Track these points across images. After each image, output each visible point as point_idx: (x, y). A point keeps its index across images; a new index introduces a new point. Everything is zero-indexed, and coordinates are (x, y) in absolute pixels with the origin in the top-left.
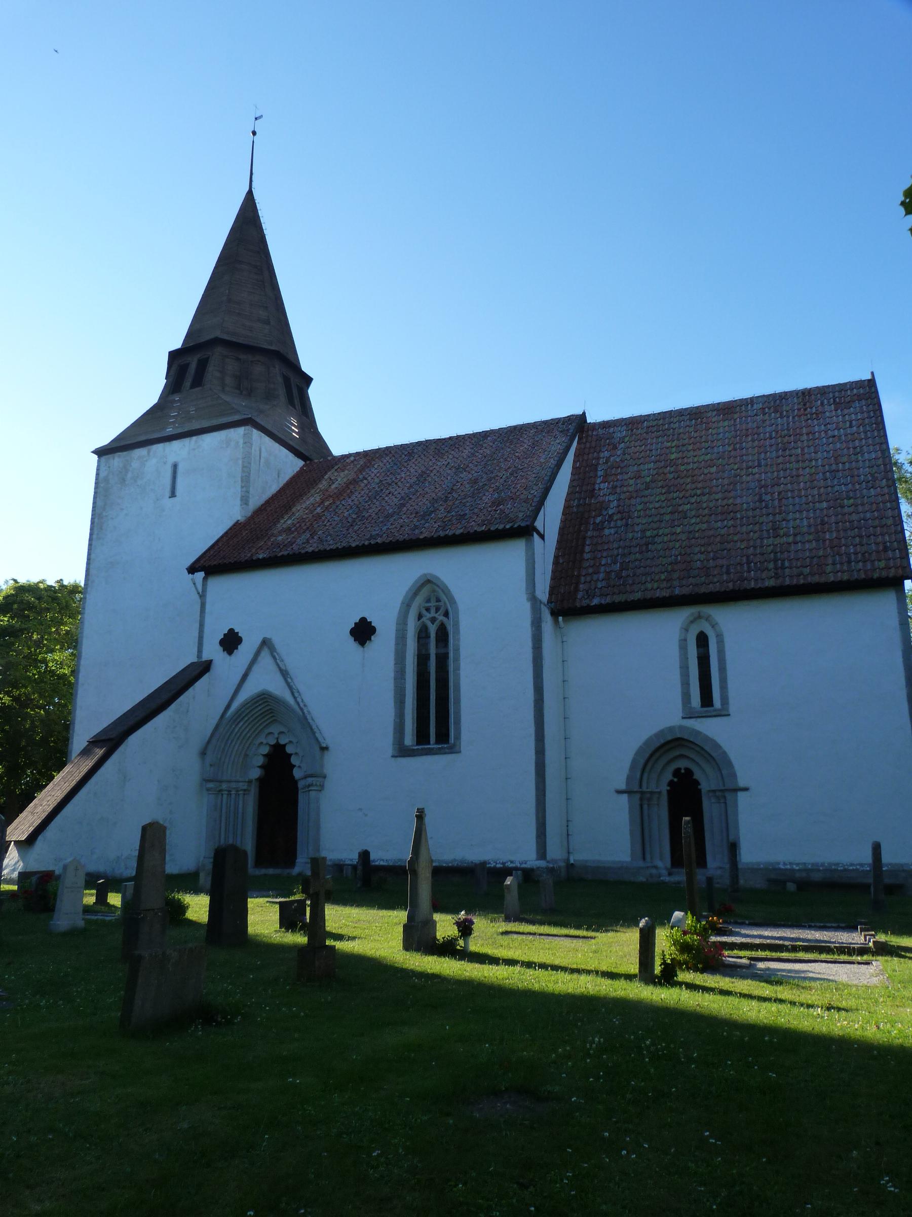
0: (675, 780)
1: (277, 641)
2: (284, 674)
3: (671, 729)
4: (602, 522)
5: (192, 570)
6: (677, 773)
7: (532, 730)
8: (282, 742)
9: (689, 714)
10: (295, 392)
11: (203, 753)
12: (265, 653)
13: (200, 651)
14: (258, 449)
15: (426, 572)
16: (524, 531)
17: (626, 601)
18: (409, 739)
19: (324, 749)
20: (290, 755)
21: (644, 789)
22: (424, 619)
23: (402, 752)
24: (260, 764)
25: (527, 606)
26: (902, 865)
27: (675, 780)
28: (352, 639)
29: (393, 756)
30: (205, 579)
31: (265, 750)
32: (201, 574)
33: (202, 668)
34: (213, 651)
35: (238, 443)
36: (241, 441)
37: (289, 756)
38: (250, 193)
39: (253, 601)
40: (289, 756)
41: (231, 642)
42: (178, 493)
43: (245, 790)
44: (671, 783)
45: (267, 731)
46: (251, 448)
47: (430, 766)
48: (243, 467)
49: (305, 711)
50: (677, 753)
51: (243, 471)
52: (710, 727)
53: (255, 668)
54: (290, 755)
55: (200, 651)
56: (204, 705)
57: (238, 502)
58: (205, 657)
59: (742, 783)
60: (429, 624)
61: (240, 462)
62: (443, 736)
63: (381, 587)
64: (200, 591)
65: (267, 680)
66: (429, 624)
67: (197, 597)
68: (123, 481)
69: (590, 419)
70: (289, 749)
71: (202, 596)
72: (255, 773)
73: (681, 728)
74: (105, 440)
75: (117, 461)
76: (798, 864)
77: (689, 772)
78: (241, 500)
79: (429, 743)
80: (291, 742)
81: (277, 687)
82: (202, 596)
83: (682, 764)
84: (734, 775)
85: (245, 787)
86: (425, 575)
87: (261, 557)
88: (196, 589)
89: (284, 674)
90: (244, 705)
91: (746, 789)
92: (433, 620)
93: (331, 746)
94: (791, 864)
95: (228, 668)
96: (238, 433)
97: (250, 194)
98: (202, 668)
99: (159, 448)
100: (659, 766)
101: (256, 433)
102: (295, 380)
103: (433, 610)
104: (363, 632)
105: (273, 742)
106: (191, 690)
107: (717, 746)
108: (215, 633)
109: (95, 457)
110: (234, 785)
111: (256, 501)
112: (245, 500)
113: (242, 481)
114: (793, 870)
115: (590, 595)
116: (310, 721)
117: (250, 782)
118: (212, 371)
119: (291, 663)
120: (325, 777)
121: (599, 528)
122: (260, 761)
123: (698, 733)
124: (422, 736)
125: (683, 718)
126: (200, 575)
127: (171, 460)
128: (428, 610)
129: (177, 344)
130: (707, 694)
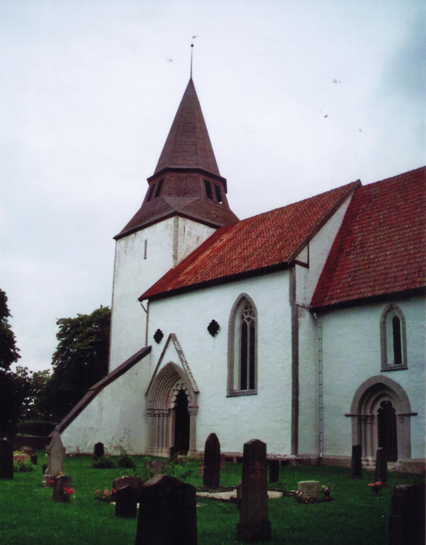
0: (382, 408)
2: (180, 352)
3: (375, 378)
4: (350, 251)
5: (141, 299)
7: (290, 381)
8: (184, 388)
9: (386, 368)
10: (213, 190)
11: (147, 395)
12: (171, 342)
13: (147, 342)
14: (183, 227)
16: (284, 266)
17: (342, 302)
18: (236, 387)
19: (197, 393)
20: (187, 396)
21: (363, 414)
22: (244, 319)
23: (232, 394)
24: (174, 401)
27: (382, 408)
28: (208, 332)
29: (227, 397)
30: (148, 304)
31: (176, 393)
32: (147, 301)
33: (147, 351)
34: (152, 342)
35: (171, 226)
36: (173, 225)
37: (186, 396)
38: (191, 82)
40: (186, 396)
41: (159, 336)
42: (147, 256)
43: (167, 414)
45: (176, 383)
46: (178, 228)
47: (244, 402)
48: (174, 239)
49: (188, 372)
50: (381, 392)
51: (174, 241)
52: (397, 377)
53: (167, 350)
54: (187, 396)
55: (147, 342)
56: (146, 370)
57: (172, 258)
58: (149, 345)
60: (246, 321)
61: (172, 236)
62: (253, 386)
63: (219, 303)
64: (146, 309)
65: (171, 357)
66: (246, 321)
67: (145, 312)
68: (126, 251)
69: (364, 183)
70: (187, 393)
71: (147, 312)
72: (172, 405)
73: (381, 377)
74: (118, 231)
75: (122, 242)
77: (390, 404)
78: (173, 257)
79: (246, 389)
80: (186, 389)
81: (176, 360)
82: (147, 312)
83: (386, 399)
84: (409, 406)
85: (167, 413)
86: (242, 294)
87: (168, 290)
88: (144, 309)
89: (180, 352)
90: (163, 370)
92: (249, 319)
93: (201, 391)
95: (157, 349)
96: (171, 221)
97: (191, 82)
98: (147, 351)
99: (139, 233)
100: (371, 402)
101: (180, 219)
102: (212, 182)
103: (248, 313)
104: (213, 328)
105: (179, 388)
106: (139, 363)
107: (399, 387)
109: (115, 240)
110: (161, 412)
111: (182, 256)
112: (175, 257)
113: (173, 247)
115: (331, 299)
116: (190, 378)
117: (170, 410)
118: (165, 187)
120: (197, 408)
121: (348, 254)
122: (174, 399)
123: (390, 380)
124: (243, 386)
125: (382, 371)
126: (145, 302)
127: (144, 238)
128: (246, 313)
129: (151, 173)
130: (397, 354)
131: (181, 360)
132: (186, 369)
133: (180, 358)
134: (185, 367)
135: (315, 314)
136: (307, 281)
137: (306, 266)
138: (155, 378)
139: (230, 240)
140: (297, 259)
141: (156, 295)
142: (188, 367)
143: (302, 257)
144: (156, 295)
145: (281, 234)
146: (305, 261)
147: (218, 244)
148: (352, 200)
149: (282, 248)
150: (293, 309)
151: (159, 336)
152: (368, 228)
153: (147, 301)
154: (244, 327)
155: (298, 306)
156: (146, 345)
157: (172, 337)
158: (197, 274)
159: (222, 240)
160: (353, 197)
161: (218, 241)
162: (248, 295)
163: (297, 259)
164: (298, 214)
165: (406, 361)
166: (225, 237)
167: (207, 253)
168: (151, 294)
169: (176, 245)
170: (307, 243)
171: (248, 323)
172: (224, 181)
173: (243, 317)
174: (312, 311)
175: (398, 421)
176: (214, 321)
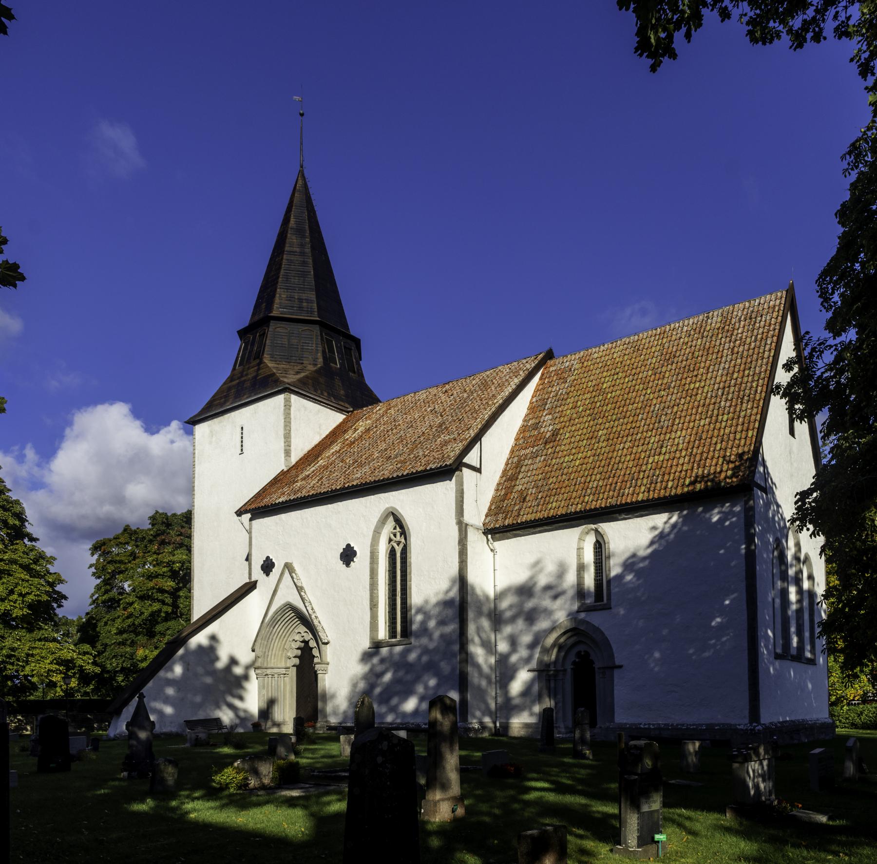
1: (296, 566)
2: (300, 589)
5: (239, 513)
6: (578, 654)
15: (387, 506)
25: (456, 528)
26: (731, 725)
30: (251, 520)
32: (249, 515)
33: (250, 587)
39: (279, 534)
41: (268, 567)
44: (574, 663)
49: (313, 617)
59: (617, 663)
60: (395, 545)
64: (248, 528)
65: (287, 595)
66: (395, 545)
71: (250, 532)
76: (653, 725)
77: (587, 654)
79: (395, 637)
82: (250, 532)
84: (611, 656)
89: (300, 589)
91: (620, 667)
94: (649, 724)
104: (348, 555)
108: (258, 562)
112: (288, 453)
114: (649, 729)
119: (304, 582)
131: (303, 599)
132: (311, 611)
133: (301, 596)
134: (309, 608)
135: (490, 536)
136: (480, 488)
137: (478, 470)
138: (265, 624)
139: (368, 430)
140: (465, 460)
141: (260, 508)
142: (312, 609)
143: (472, 458)
144: (260, 508)
145: (440, 425)
146: (476, 464)
147: (350, 435)
148: (541, 379)
149: (446, 443)
150: (460, 530)
151: (268, 567)
152: (562, 419)
153: (249, 515)
154: (392, 553)
155: (467, 525)
156: (250, 578)
157: (288, 567)
158: (321, 478)
159: (356, 430)
160: (543, 374)
161: (350, 432)
162: (397, 510)
163: (465, 460)
164: (465, 395)
165: (609, 598)
166: (362, 425)
167: (336, 448)
168: (253, 506)
169: (287, 437)
170: (477, 438)
171: (398, 550)
172: (357, 342)
173: (390, 540)
174: (485, 533)
175: (598, 677)
176: (348, 545)
